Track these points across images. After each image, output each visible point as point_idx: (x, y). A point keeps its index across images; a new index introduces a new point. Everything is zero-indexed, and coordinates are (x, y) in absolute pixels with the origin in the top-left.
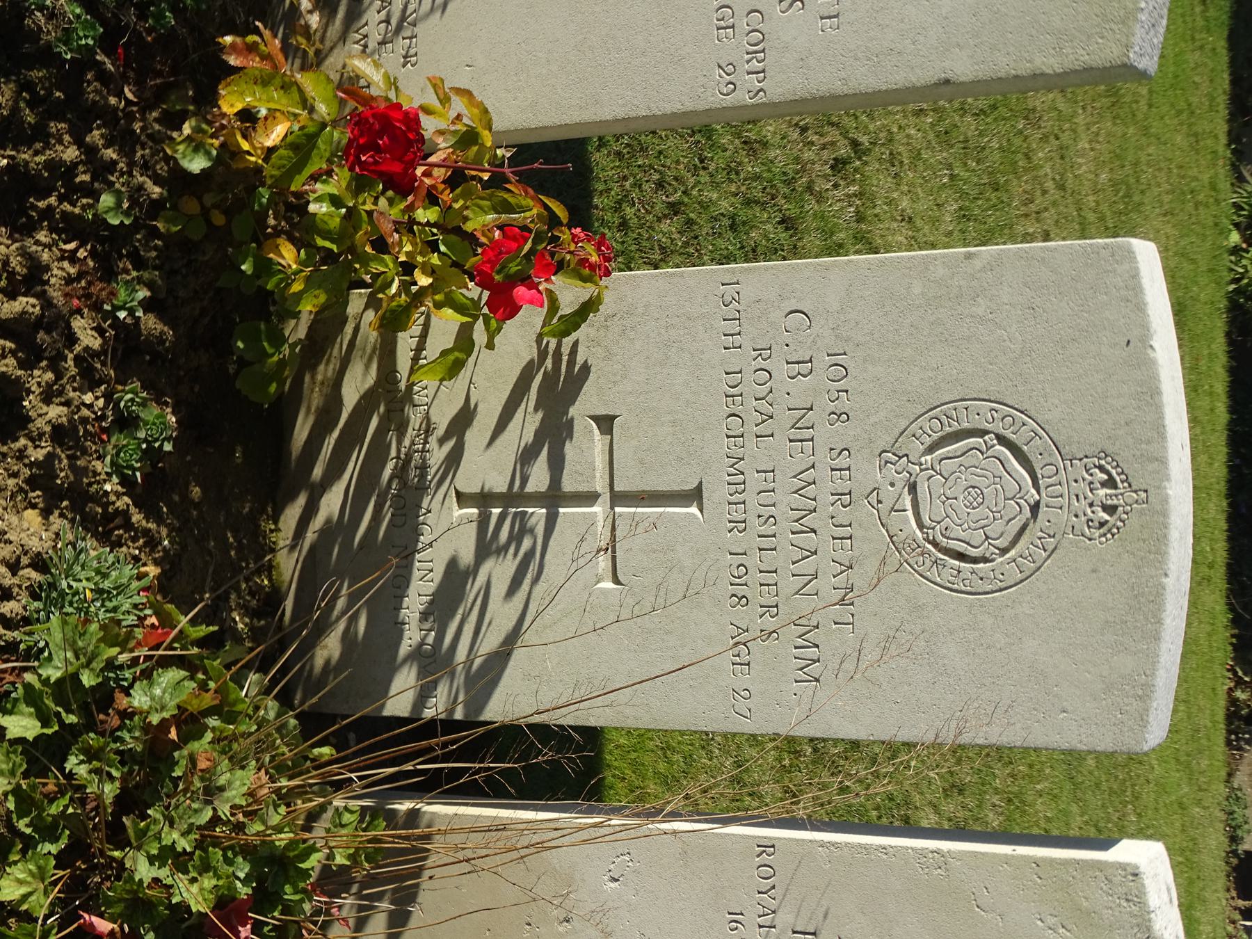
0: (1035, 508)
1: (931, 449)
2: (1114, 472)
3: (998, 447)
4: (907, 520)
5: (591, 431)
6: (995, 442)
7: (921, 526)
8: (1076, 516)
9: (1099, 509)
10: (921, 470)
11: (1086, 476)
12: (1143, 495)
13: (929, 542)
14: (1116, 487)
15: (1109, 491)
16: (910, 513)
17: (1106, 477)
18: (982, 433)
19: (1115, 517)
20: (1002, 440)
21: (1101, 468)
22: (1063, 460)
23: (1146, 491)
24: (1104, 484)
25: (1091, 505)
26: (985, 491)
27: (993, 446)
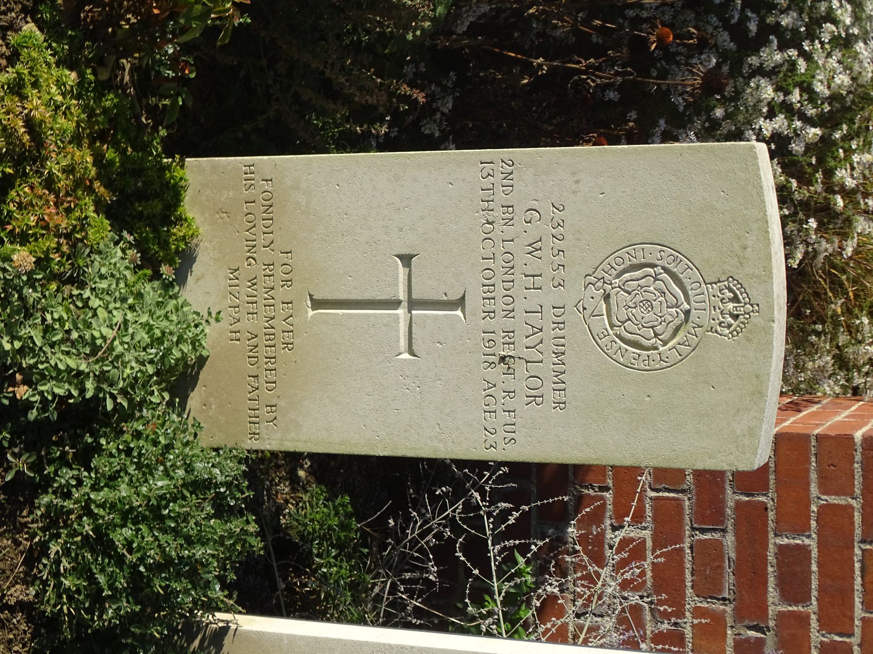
0: (687, 313)
1: (618, 276)
2: (738, 292)
4: (603, 320)
5: (397, 269)
6: (662, 271)
7: (612, 326)
8: (714, 320)
9: (728, 316)
10: (613, 288)
11: (719, 295)
13: (617, 337)
14: (739, 301)
16: (605, 317)
17: (732, 295)
18: (652, 266)
19: (737, 322)
20: (666, 270)
21: (731, 290)
22: (706, 284)
23: (758, 305)
26: (654, 303)
27: (661, 274)
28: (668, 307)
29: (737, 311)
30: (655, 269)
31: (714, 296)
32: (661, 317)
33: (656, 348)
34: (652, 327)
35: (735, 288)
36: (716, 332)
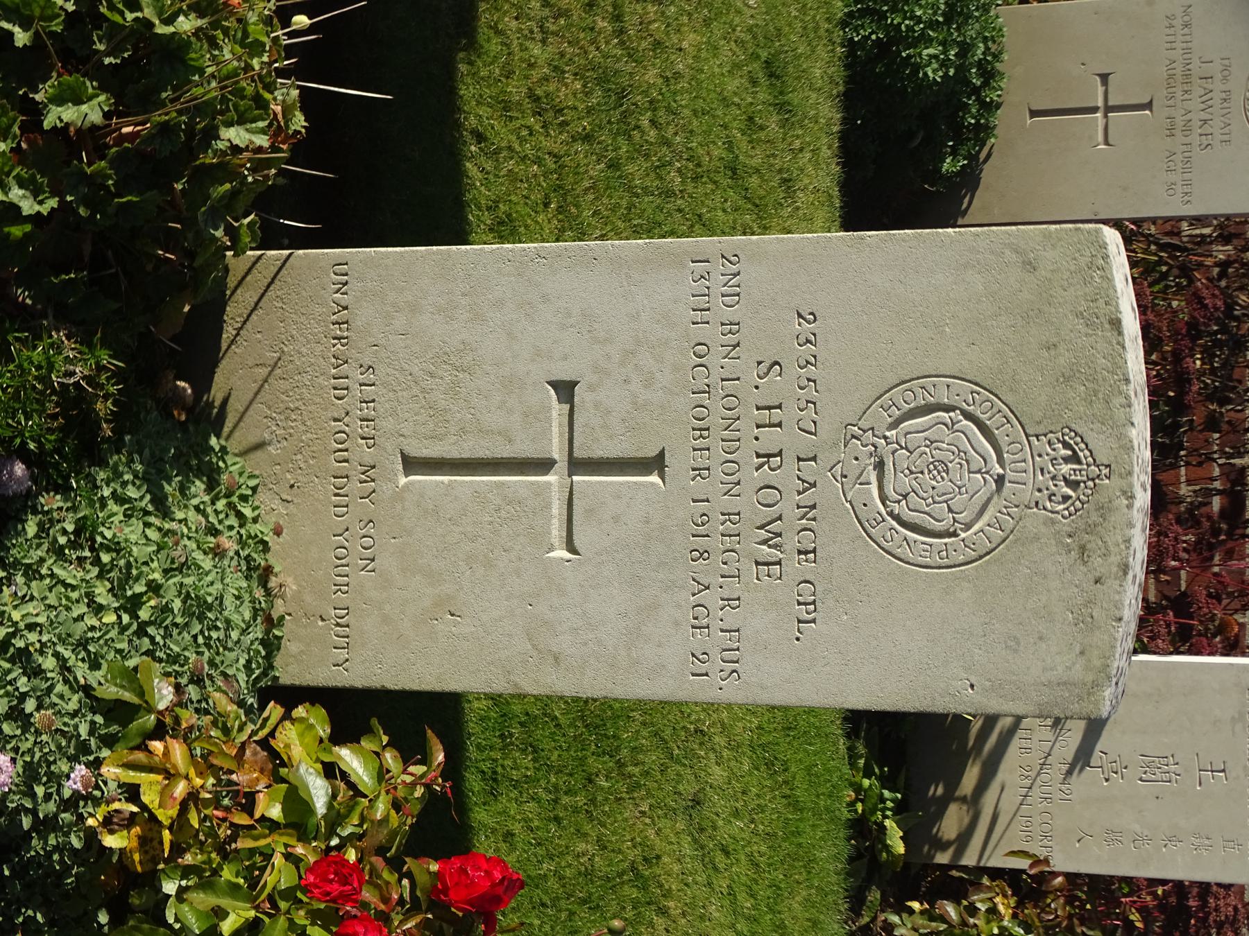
0: (1000, 480)
1: (894, 425)
3: (965, 422)
4: (869, 492)
6: (961, 417)
9: (1063, 483)
12: (1105, 471)
14: (1080, 462)
15: (1075, 466)
17: (1070, 453)
18: (948, 409)
20: (968, 416)
21: (1066, 445)
22: (1027, 436)
24: (1066, 460)
25: (1053, 478)
28: (970, 472)
29: (1075, 475)
30: (952, 414)
31: (1040, 456)
32: (959, 488)
33: (955, 534)
34: (946, 502)
35: (1072, 442)
36: (1045, 509)
